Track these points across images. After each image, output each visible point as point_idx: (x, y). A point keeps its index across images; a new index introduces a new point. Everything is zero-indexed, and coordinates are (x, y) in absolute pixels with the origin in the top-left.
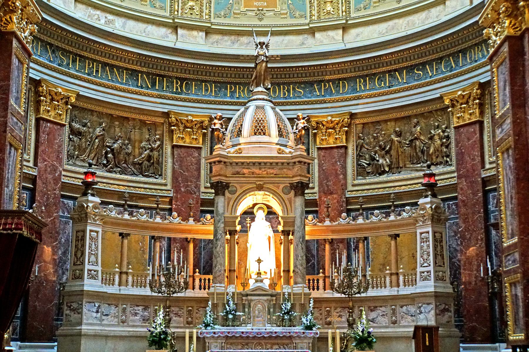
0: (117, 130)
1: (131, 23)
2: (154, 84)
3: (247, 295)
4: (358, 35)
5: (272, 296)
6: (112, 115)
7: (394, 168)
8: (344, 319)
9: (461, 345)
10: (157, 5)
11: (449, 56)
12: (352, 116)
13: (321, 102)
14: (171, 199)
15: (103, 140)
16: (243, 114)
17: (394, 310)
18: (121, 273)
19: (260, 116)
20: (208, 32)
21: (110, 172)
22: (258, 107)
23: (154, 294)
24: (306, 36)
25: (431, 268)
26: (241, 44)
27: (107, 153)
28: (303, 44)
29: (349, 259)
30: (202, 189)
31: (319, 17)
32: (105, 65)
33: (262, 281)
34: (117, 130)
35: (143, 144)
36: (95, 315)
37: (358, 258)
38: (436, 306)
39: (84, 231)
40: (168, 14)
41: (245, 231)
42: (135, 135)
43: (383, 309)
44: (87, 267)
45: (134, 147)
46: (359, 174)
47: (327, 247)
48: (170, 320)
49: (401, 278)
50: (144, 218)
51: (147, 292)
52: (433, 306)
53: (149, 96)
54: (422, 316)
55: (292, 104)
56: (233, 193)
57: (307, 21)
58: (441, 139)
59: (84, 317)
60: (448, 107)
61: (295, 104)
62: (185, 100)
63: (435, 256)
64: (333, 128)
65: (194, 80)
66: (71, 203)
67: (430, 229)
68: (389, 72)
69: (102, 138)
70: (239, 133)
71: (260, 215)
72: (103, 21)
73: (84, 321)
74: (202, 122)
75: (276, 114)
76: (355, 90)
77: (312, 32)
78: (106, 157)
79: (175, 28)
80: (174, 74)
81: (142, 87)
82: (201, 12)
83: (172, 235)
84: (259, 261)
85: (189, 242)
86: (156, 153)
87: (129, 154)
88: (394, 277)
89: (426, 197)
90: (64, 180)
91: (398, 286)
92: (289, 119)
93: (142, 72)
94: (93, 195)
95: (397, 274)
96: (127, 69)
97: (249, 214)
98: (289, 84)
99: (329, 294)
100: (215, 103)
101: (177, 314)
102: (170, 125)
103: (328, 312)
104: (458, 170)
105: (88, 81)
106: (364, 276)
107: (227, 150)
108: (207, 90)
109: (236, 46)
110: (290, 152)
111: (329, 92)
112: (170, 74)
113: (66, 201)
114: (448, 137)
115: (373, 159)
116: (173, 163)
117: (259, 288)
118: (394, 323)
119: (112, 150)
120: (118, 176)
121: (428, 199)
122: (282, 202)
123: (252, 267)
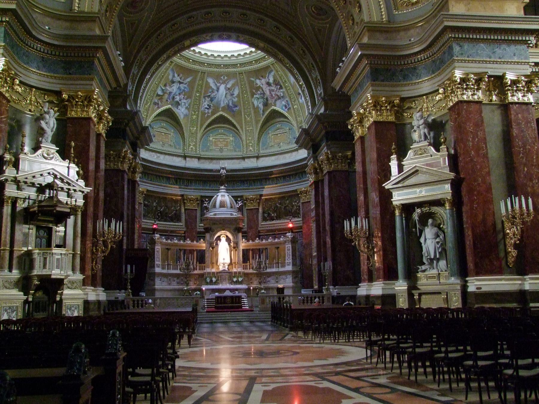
0: (162, 203)
1: (167, 157)
2: (177, 183)
3: (220, 273)
4: (263, 161)
5: (229, 273)
6: (159, 197)
7: (278, 218)
8: (258, 281)
9: (302, 290)
10: (178, 147)
11: (299, 173)
12: (261, 195)
13: (247, 189)
14: (185, 231)
15: (156, 208)
16: (216, 198)
17: (277, 277)
18: (168, 265)
19: (223, 198)
20: (199, 158)
21: (160, 221)
22: (222, 196)
23: (181, 273)
24: (241, 160)
25: (291, 261)
26: (213, 164)
27: (158, 213)
28: (239, 163)
29: (260, 257)
30: (198, 227)
31: (247, 152)
32: (156, 176)
33: (225, 267)
34: (162, 203)
35: (173, 208)
36: (159, 282)
37: (263, 257)
38: (293, 276)
39: (154, 249)
40: (181, 151)
41: (217, 244)
42: (169, 205)
43: (273, 277)
44: (156, 263)
45: (169, 209)
46: (263, 220)
47: (251, 252)
48: (188, 283)
49: (280, 264)
50: (176, 242)
51: (178, 272)
52: (291, 276)
53: (175, 188)
54: (287, 279)
55: (235, 190)
56: (213, 231)
57: (241, 153)
58: (297, 207)
59: (156, 283)
60: (299, 194)
61: (237, 190)
62: (190, 189)
63: (293, 256)
64: (253, 200)
65: (193, 180)
66: (145, 235)
67: (290, 246)
68: (276, 177)
69: (156, 207)
70: (214, 206)
71: (223, 239)
72: (155, 157)
73: (156, 284)
74: (197, 198)
75: (229, 197)
76: (261, 185)
77: (244, 158)
78: (158, 215)
79: (185, 157)
80: (185, 178)
81: (172, 184)
82: (196, 149)
83: (185, 248)
84: (224, 259)
85: (194, 251)
86: (178, 212)
87: (167, 213)
88: (277, 265)
89: (289, 232)
90: (143, 226)
91: (279, 268)
92: (235, 201)
93: (172, 178)
94: (157, 234)
95: (278, 263)
96: (166, 177)
97: (219, 238)
98: (234, 181)
99: (251, 271)
100: (203, 190)
101: (190, 280)
102: (184, 200)
103: (251, 278)
104: (303, 220)
105: (151, 184)
106: (265, 264)
107: (210, 214)
108: (199, 184)
109: (211, 165)
110: (236, 215)
111: (251, 185)
112: (183, 178)
113: (143, 235)
114: (299, 206)
115: (269, 214)
116: (185, 216)
117: (224, 270)
118: (277, 282)
119: (160, 212)
120: (163, 223)
121: (290, 234)
122: (233, 235)
123: (221, 260)
